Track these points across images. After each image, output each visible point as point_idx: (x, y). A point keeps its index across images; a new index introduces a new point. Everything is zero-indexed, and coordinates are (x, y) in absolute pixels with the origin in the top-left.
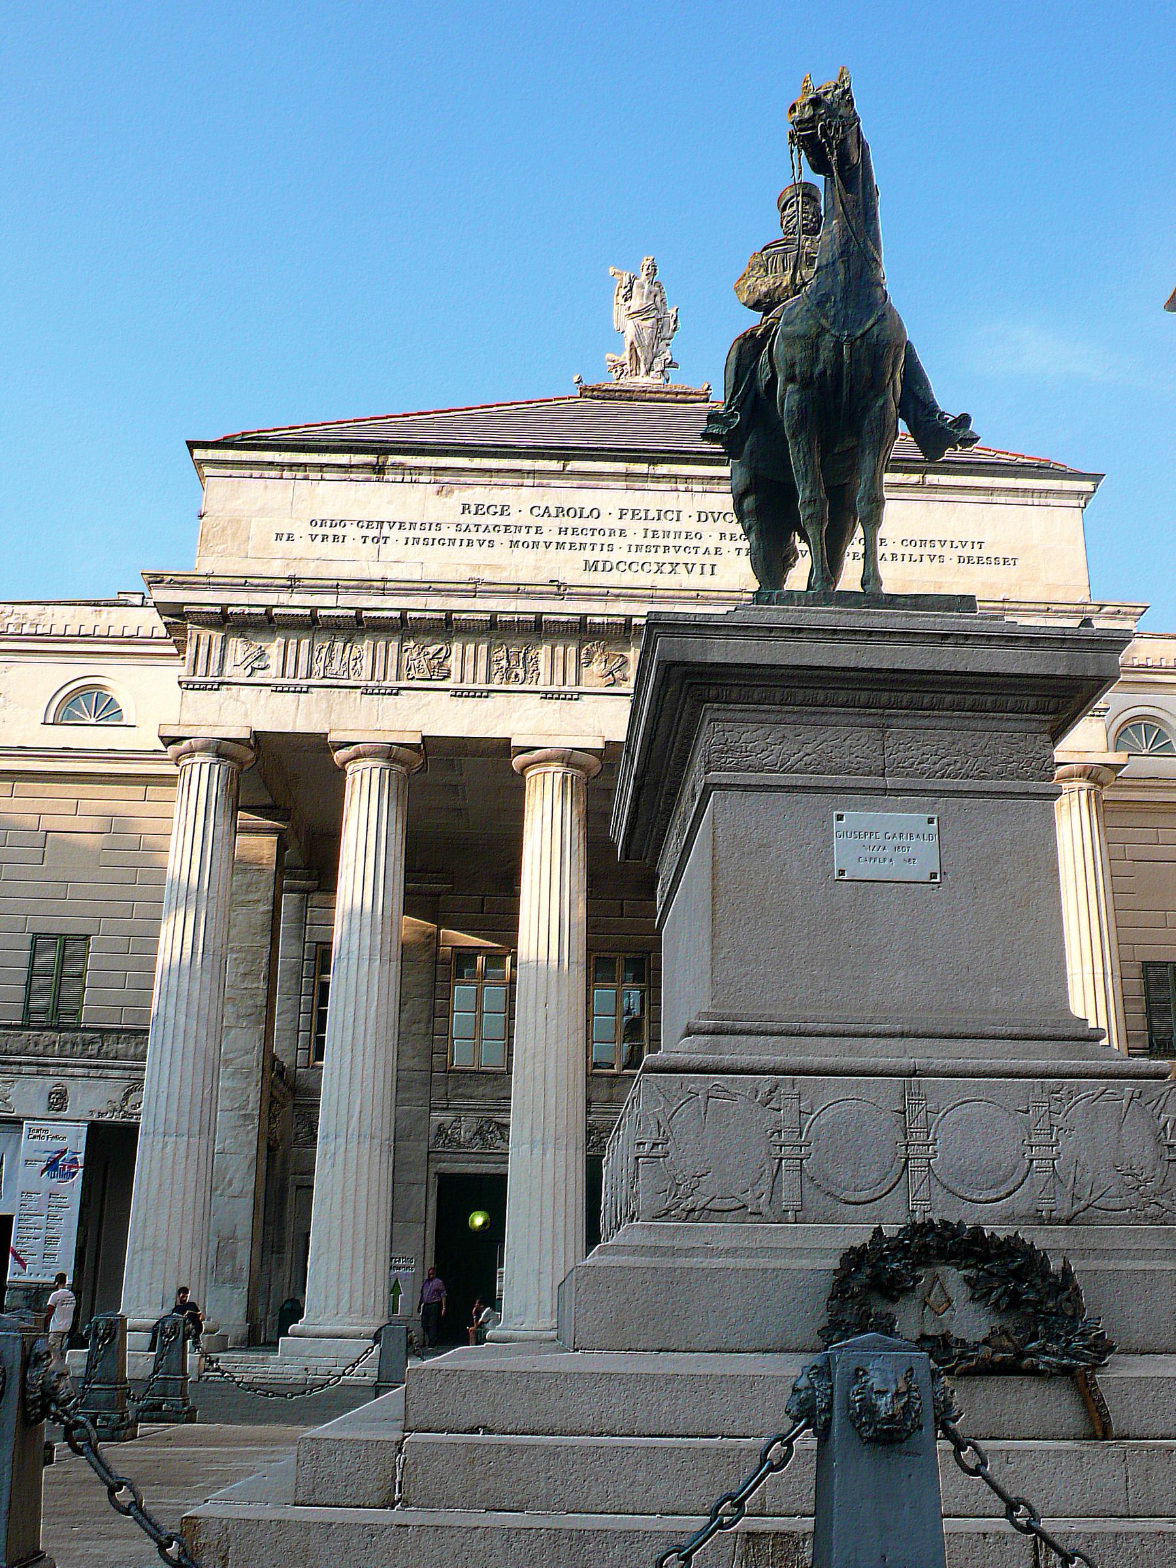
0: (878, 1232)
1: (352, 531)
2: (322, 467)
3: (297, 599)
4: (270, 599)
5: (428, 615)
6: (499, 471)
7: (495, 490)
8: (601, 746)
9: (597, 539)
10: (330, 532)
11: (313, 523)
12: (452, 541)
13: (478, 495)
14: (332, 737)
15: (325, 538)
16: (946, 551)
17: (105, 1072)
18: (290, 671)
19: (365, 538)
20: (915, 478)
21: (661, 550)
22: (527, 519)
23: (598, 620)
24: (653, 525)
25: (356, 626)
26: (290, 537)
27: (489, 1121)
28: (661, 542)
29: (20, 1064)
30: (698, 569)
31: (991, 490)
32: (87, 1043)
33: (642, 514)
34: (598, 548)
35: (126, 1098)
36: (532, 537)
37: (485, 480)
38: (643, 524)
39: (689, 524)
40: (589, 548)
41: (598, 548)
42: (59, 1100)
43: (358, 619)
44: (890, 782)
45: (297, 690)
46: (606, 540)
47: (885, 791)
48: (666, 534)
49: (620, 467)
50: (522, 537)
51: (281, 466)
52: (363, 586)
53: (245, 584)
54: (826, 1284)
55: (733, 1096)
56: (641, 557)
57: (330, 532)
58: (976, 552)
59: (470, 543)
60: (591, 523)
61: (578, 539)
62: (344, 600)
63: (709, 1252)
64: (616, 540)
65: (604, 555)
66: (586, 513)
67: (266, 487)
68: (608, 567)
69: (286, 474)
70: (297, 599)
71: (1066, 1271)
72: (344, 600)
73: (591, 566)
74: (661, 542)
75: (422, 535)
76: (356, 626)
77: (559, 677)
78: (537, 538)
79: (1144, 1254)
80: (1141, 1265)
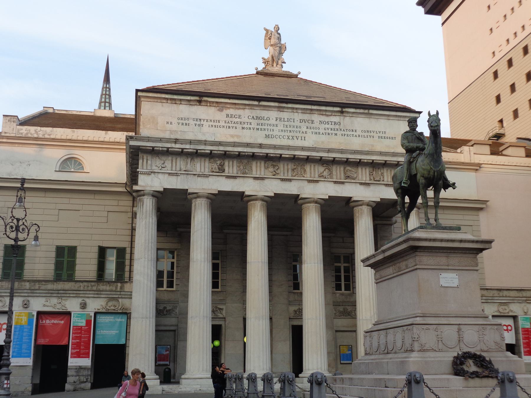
0: (458, 354)
1: (192, 122)
2: (181, 100)
3: (178, 146)
4: (168, 145)
5: (219, 152)
6: (238, 104)
7: (237, 110)
8: (273, 195)
9: (269, 127)
10: (184, 122)
11: (178, 119)
12: (223, 126)
13: (231, 111)
14: (189, 191)
15: (183, 124)
16: (375, 134)
17: (99, 296)
18: (174, 169)
19: (196, 124)
20: (366, 111)
21: (289, 131)
22: (246, 120)
23: (272, 155)
24: (286, 123)
25: (196, 155)
26: (171, 123)
27: (216, 307)
28: (289, 129)
29: (70, 294)
30: (300, 138)
31: (388, 116)
32: (92, 286)
33: (283, 120)
34: (269, 130)
35: (107, 304)
36: (249, 126)
37: (234, 106)
38: (283, 122)
39: (297, 123)
40: (266, 130)
41: (269, 130)
42: (84, 306)
43: (197, 152)
44: (450, 268)
45: (176, 175)
46: (272, 128)
47: (449, 269)
48: (290, 126)
49: (276, 104)
50: (245, 126)
51: (167, 99)
52: (199, 142)
53: (161, 140)
54: (451, 363)
55: (429, 329)
56: (283, 134)
57: (184, 122)
58: (383, 135)
59: (229, 127)
60: (267, 122)
61: (263, 127)
62: (192, 147)
63: (430, 357)
64: (275, 128)
65: (271, 133)
66: (265, 118)
67: (162, 106)
68: (272, 137)
69: (169, 101)
70: (178, 146)
71: (490, 360)
72: (192, 147)
73: (267, 136)
74: (289, 129)
75: (214, 124)
76: (196, 155)
77: (258, 173)
78: (250, 126)
79: (501, 357)
80: (501, 359)
